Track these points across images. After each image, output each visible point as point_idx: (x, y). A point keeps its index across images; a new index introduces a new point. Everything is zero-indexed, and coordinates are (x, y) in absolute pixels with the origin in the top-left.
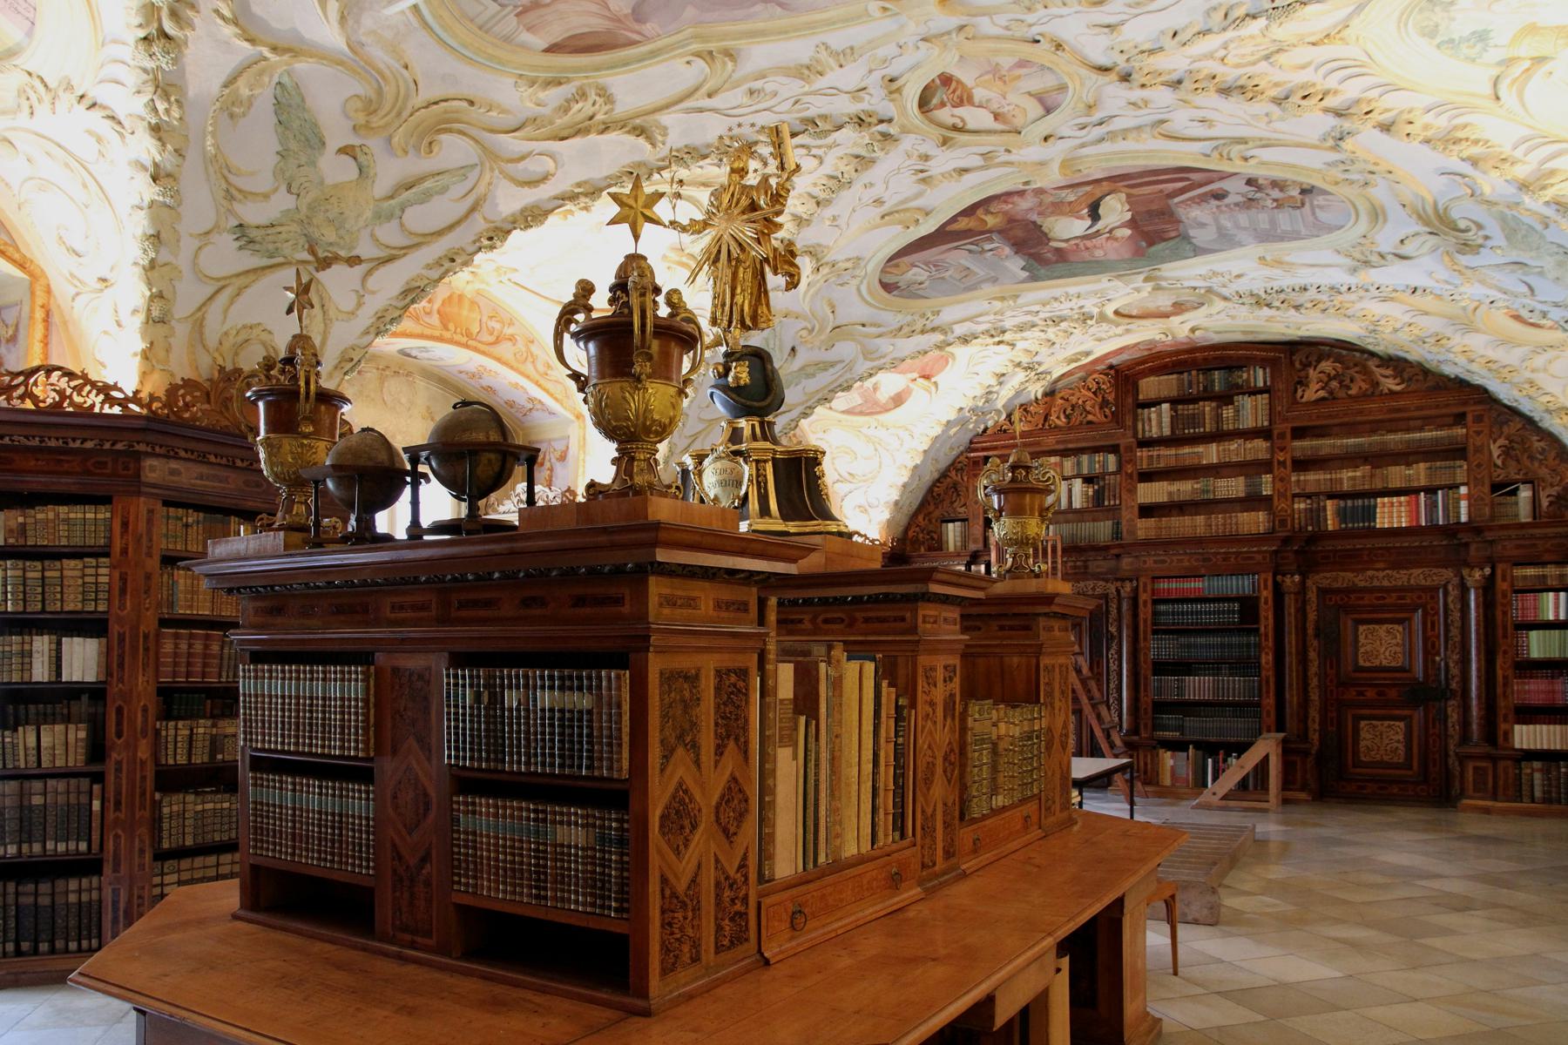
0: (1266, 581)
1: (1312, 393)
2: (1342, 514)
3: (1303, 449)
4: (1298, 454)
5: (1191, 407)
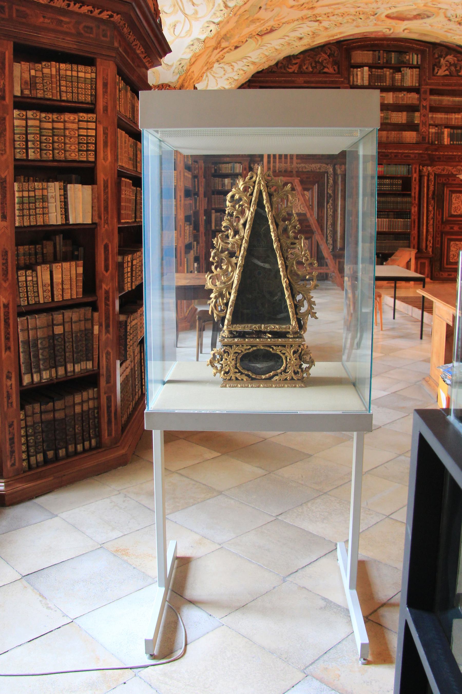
0: (415, 169)
1: (441, 72)
2: (451, 136)
3: (449, 101)
4: (433, 104)
5: (379, 71)
